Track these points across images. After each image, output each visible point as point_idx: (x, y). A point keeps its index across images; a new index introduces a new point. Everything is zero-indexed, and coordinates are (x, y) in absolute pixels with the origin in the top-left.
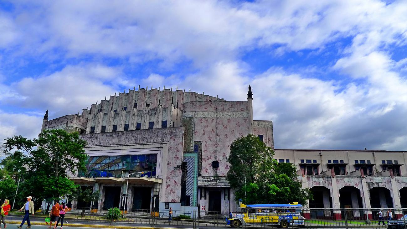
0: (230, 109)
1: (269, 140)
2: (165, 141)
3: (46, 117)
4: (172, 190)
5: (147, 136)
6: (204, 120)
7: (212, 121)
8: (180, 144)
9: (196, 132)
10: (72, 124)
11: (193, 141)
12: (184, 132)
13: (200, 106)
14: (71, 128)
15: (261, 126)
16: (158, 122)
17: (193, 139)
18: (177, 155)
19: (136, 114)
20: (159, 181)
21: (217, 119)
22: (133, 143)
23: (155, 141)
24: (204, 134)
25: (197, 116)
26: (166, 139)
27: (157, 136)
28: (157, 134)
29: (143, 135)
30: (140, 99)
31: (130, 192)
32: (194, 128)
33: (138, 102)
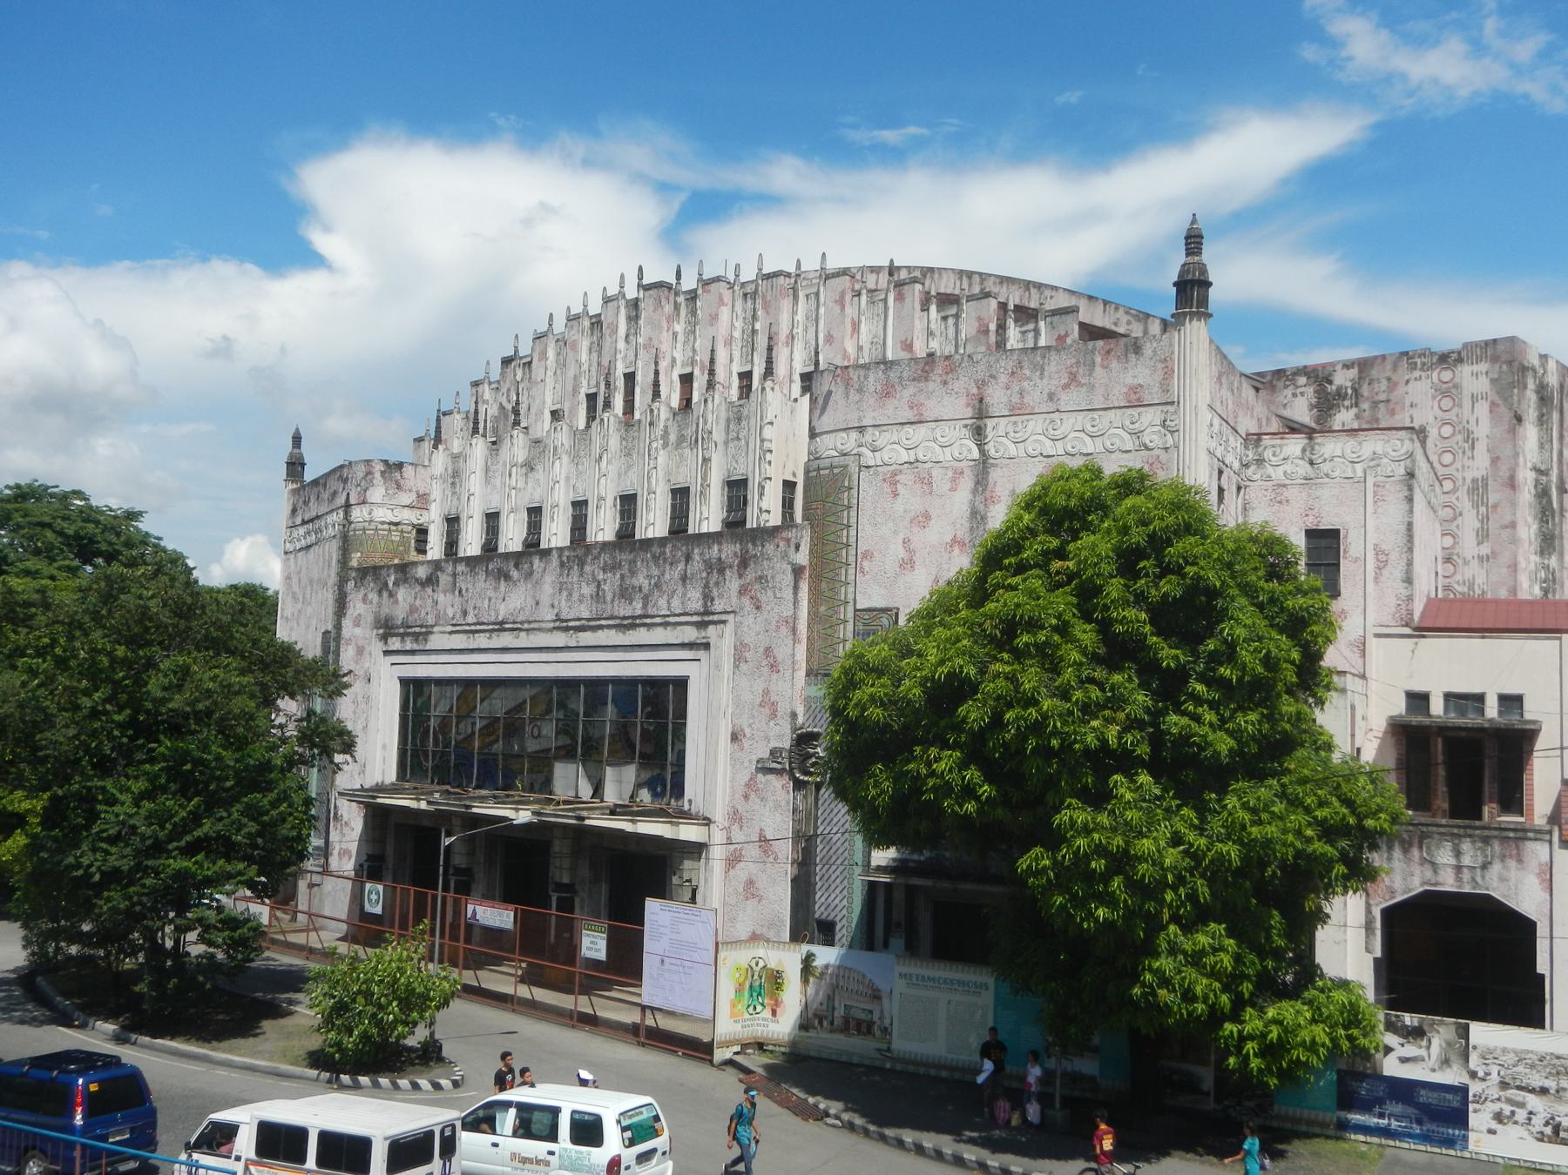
0: (1063, 396)
1: (1382, 565)
2: (718, 606)
3: (295, 467)
4: (750, 883)
5: (641, 580)
6: (906, 478)
7: (954, 480)
8: (784, 630)
9: (868, 555)
10: (365, 509)
11: (850, 609)
12: (802, 558)
13: (887, 392)
14: (364, 530)
15: (1326, 467)
16: (705, 486)
17: (850, 597)
18: (773, 688)
19: (614, 442)
20: (688, 833)
21: (983, 465)
22: (586, 614)
23: (676, 605)
24: (908, 564)
25: (869, 458)
26: (721, 596)
27: (684, 578)
28: (681, 566)
29: (625, 570)
30: (645, 347)
31: (585, 871)
32: (853, 532)
33: (640, 364)
